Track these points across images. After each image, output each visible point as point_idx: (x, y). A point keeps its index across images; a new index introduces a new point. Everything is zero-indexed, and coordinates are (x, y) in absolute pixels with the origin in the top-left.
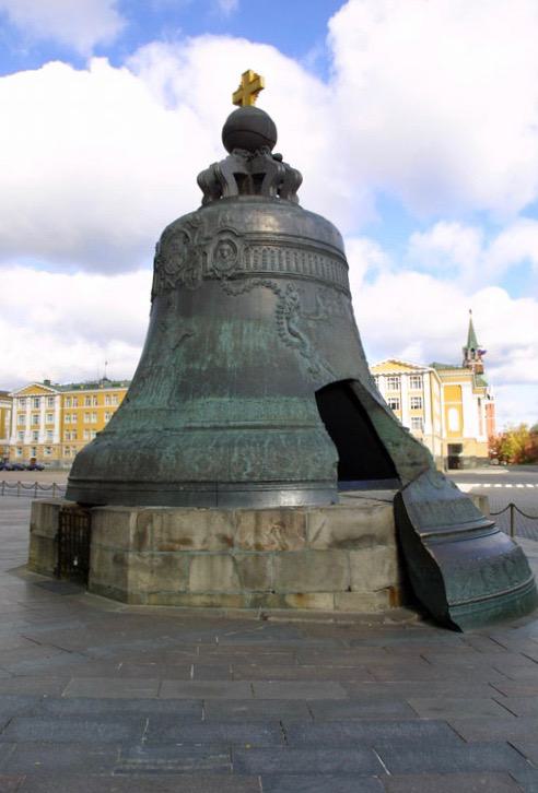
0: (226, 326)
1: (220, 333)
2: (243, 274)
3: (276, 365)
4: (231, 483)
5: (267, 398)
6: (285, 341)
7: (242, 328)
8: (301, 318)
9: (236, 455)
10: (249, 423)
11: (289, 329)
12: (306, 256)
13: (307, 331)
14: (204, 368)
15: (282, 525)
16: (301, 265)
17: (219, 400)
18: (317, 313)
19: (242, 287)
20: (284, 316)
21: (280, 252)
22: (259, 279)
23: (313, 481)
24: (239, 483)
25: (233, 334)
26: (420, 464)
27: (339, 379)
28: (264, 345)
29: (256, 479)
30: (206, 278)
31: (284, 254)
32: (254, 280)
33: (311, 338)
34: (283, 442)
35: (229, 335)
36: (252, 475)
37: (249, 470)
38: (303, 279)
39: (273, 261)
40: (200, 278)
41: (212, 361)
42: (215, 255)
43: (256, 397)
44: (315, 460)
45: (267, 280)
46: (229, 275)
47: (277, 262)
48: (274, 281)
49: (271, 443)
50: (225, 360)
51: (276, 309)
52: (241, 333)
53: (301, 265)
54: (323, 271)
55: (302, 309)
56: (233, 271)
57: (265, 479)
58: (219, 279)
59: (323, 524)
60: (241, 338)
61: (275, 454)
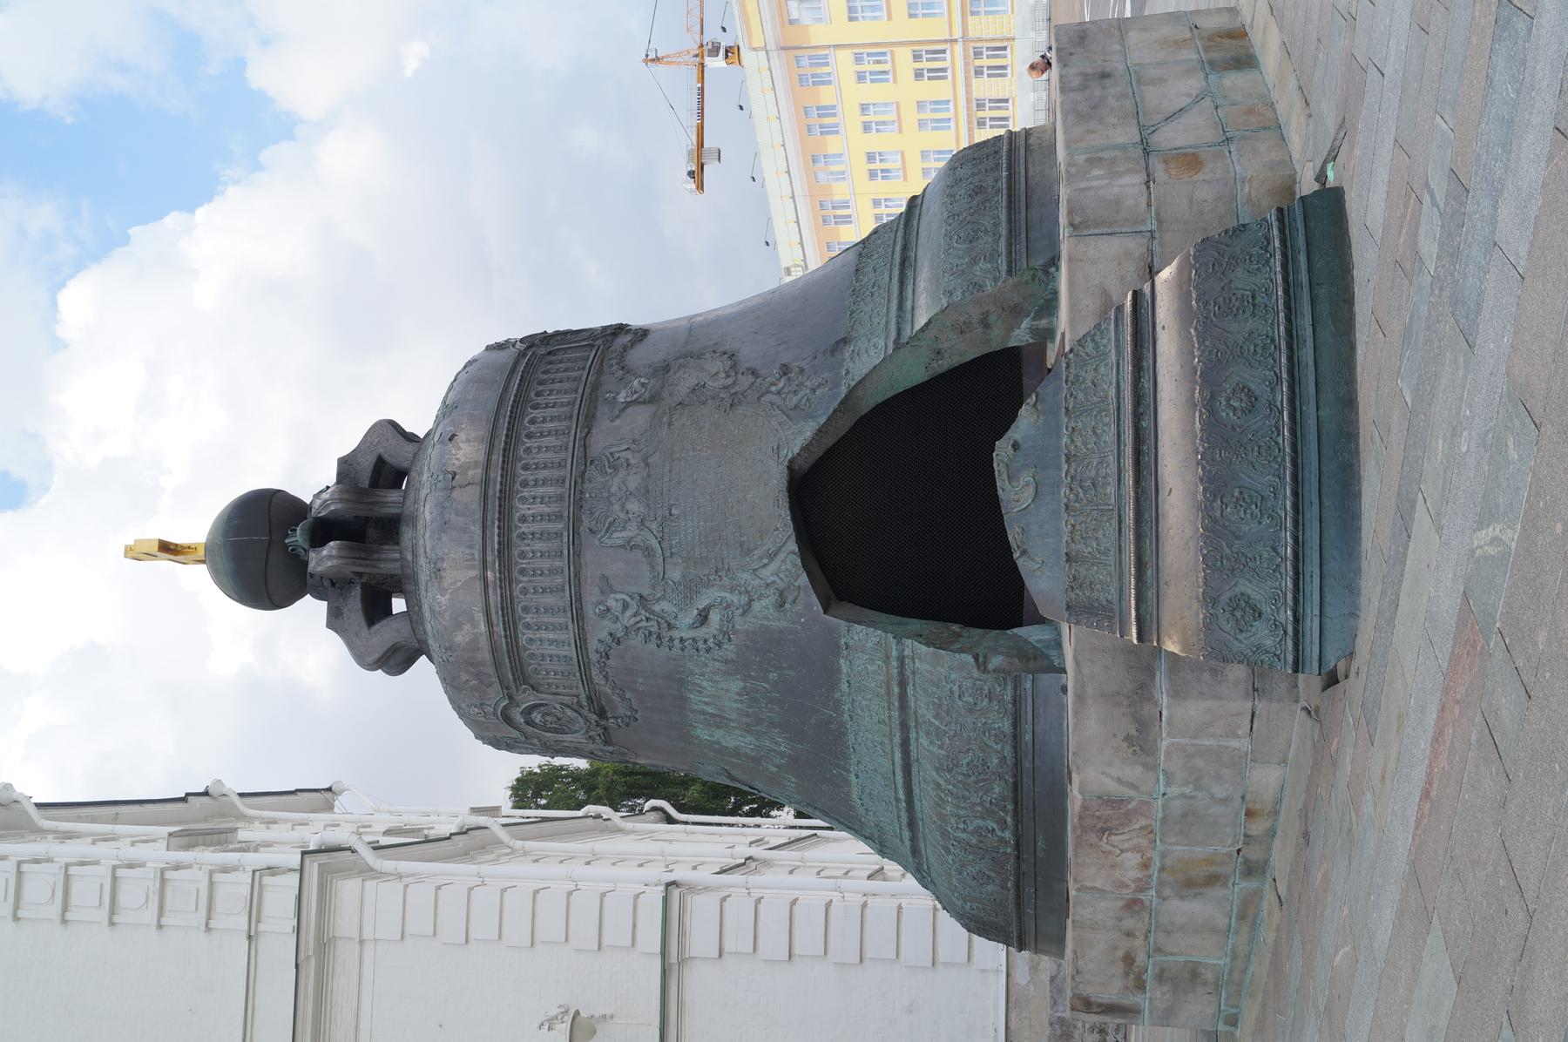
0: (703, 733)
1: (718, 743)
2: (589, 698)
3: (773, 676)
4: (1018, 857)
5: (846, 717)
6: (719, 645)
7: (703, 712)
8: (663, 598)
9: (964, 836)
10: (900, 779)
11: (692, 627)
12: (524, 564)
13: (690, 589)
14: (793, 780)
15: (1103, 831)
16: (547, 581)
17: (855, 792)
18: (648, 551)
19: (615, 698)
20: (666, 634)
21: (528, 626)
22: (594, 672)
23: (1016, 724)
24: (1018, 846)
25: (718, 727)
26: (986, 315)
27: (791, 530)
28: (735, 685)
29: (1009, 819)
30: (606, 743)
31: (529, 619)
32: (598, 678)
33: (708, 585)
34: (935, 749)
35: (719, 734)
36: (1003, 825)
37: (991, 824)
38: (577, 575)
39: (552, 642)
40: (610, 749)
41: (776, 766)
42: (556, 731)
43: (845, 734)
44: (971, 710)
45: (594, 657)
46: (595, 717)
47: (551, 636)
48: (593, 644)
49: (937, 770)
50: (774, 751)
51: (652, 646)
52: (715, 715)
53: (547, 581)
54: (549, 517)
55: (646, 592)
56: (585, 712)
57: (1010, 807)
58: (605, 729)
59: (1103, 773)
60: (727, 719)
61: (960, 778)
